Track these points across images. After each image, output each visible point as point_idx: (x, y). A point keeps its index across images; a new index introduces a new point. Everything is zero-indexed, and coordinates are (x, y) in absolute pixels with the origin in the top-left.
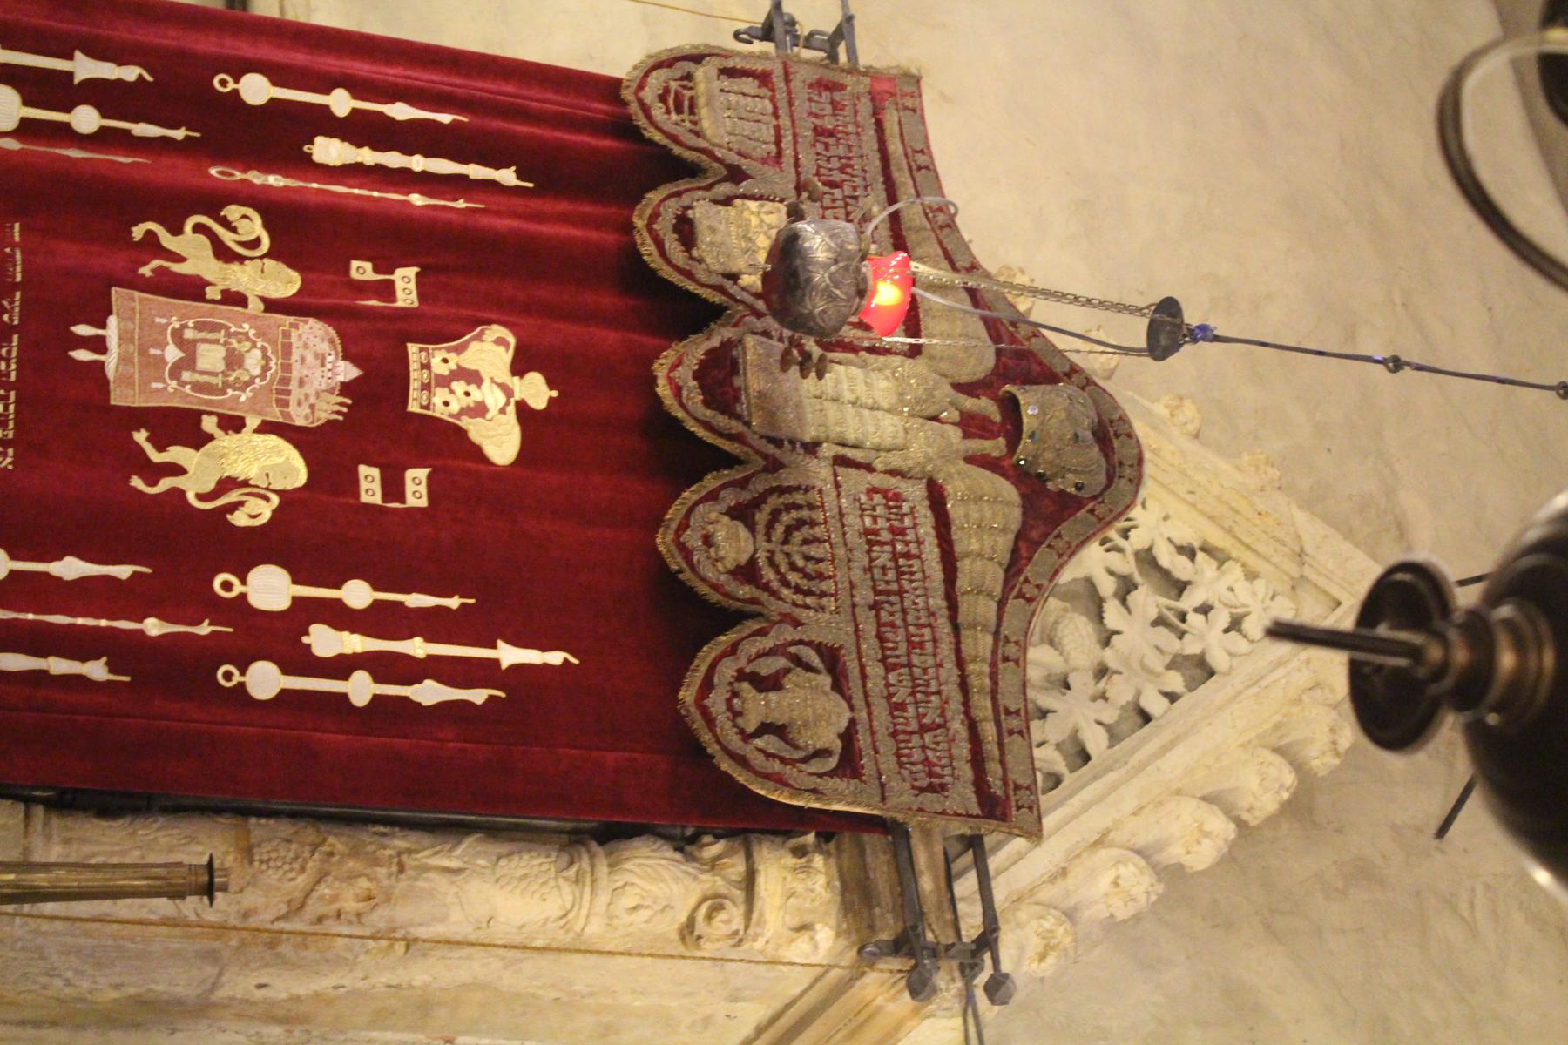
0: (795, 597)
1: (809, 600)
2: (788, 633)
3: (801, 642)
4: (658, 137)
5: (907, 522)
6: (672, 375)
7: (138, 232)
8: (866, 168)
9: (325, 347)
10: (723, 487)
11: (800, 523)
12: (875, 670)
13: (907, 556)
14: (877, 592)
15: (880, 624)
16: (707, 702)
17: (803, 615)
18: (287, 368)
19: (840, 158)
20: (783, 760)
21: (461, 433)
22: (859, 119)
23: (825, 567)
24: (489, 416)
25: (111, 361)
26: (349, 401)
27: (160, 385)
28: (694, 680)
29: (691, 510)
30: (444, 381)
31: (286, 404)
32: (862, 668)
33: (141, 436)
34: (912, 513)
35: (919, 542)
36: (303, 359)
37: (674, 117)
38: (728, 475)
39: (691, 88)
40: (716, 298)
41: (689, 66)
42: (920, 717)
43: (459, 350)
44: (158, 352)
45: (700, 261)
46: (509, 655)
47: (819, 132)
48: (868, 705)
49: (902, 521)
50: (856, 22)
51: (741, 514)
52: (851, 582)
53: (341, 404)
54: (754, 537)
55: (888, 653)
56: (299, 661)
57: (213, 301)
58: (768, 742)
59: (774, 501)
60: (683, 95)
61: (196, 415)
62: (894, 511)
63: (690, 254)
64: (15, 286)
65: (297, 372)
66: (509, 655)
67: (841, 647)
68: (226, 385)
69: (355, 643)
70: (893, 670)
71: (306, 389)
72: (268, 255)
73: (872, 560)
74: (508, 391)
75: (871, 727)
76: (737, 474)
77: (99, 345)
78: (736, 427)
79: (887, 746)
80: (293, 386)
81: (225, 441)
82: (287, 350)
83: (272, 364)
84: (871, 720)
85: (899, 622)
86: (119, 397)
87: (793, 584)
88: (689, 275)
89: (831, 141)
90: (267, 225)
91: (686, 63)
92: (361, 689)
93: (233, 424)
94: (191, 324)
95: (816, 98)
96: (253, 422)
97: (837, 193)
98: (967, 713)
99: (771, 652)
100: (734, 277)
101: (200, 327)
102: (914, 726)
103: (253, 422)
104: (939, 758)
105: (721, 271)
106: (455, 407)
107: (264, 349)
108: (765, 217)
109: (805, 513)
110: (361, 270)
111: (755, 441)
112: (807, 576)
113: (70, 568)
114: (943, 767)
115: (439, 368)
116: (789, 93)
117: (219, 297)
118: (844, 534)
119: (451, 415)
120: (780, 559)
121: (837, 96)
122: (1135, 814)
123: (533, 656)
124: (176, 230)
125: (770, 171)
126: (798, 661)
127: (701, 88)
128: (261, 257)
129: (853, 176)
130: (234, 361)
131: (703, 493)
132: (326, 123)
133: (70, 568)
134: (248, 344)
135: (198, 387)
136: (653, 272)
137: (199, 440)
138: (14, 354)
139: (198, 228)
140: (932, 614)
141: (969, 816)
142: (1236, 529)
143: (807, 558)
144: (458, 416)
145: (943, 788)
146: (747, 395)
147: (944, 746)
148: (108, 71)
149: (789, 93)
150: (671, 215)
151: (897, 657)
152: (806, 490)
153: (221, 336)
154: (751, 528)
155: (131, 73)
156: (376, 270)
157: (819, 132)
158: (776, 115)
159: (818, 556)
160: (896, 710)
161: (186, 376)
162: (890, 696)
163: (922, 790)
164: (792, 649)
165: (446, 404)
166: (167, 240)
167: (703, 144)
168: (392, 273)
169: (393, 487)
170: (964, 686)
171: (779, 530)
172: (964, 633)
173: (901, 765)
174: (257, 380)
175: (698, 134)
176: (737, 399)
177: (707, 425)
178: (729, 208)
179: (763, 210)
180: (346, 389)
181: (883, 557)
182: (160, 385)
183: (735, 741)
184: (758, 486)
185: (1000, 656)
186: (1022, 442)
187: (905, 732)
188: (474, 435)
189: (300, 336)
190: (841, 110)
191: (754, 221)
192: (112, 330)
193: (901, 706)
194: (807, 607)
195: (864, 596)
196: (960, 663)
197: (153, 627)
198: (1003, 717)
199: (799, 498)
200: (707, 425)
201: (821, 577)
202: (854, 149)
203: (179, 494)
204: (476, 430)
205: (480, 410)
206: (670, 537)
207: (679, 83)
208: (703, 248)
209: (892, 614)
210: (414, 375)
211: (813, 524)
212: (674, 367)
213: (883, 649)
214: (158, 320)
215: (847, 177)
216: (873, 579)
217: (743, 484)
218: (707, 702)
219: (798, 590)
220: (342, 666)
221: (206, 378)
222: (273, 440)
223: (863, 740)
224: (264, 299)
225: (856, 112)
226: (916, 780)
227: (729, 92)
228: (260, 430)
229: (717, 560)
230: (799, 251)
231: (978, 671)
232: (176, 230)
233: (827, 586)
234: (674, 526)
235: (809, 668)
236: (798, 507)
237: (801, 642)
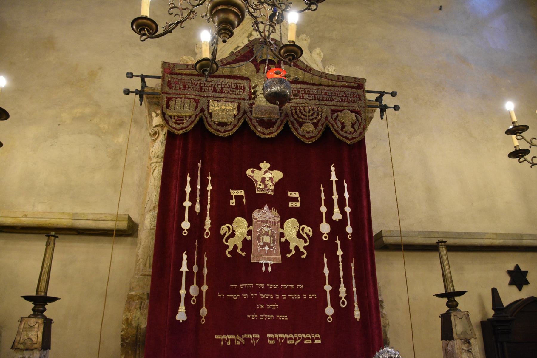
0: (319, 116)
1: (320, 113)
2: (330, 118)
3: (332, 117)
4: (192, 126)
5: (296, 89)
6: (266, 134)
7: (229, 256)
8: (195, 79)
9: (261, 212)
10: (294, 127)
11: (300, 112)
12: (334, 103)
13: (305, 91)
14: (315, 99)
15: (323, 100)
16: (350, 138)
17: (324, 115)
18: (267, 221)
19: (192, 85)
20: (360, 125)
21: (276, 183)
22: (179, 79)
23: (311, 108)
24: (273, 177)
25: (270, 262)
26: (273, 208)
27: (275, 251)
28: (345, 140)
29: (300, 135)
30: (266, 186)
31: (275, 222)
32: (334, 105)
33: (289, 256)
34: (293, 88)
35: (301, 88)
36: (264, 218)
37: (185, 121)
38: (290, 125)
39: (174, 116)
40: (242, 121)
41: (167, 116)
42: (343, 96)
43: (257, 182)
44: (267, 251)
45: (231, 122)
46: (334, 178)
47: (185, 88)
48: (343, 106)
49: (296, 91)
50: (143, 74)
51: (301, 124)
52: (313, 104)
53: (274, 210)
54: (306, 122)
55: (330, 100)
56: (343, 222)
57: (251, 238)
58: (356, 127)
59: (296, 116)
60: (177, 119)
61: (281, 243)
62: (293, 92)
63: (229, 124)
64: (254, 285)
65: (267, 219)
66: (334, 178)
67: (330, 109)
68: (272, 236)
69: (336, 210)
70: (333, 99)
71: (271, 218)
72: (231, 224)
73: (308, 99)
74: (266, 172)
75: (348, 106)
76: (290, 123)
77: (267, 265)
78: (279, 121)
79: (353, 105)
80: (270, 220)
81: (287, 237)
82: (262, 221)
83: (266, 225)
84: (346, 106)
85: (322, 96)
86: (278, 259)
87: (316, 116)
88: (235, 126)
89: (187, 86)
90: (224, 225)
91: (166, 117)
92: (348, 209)
93: (282, 235)
94: (259, 243)
95: (174, 88)
96: (281, 230)
97: (203, 88)
98: (341, 87)
99: (336, 123)
100: (235, 116)
101: (259, 241)
102: (346, 98)
103: (281, 230)
104: (352, 95)
105: (234, 118)
106: (271, 184)
107: (263, 226)
108: (215, 106)
109: (298, 111)
110: (233, 202)
111: (282, 118)
112: (314, 113)
113: (326, 271)
114: (354, 95)
115: (262, 186)
116: (173, 94)
117: (250, 237)
118: (301, 103)
119: (273, 185)
120: (311, 118)
121: (172, 82)
122: (318, 65)
123: (333, 173)
124: (227, 247)
125: (200, 103)
126: (336, 118)
127: (175, 114)
128: (232, 226)
129: (197, 83)
130: (267, 234)
131: (295, 131)
132: (192, 208)
133: (326, 271)
134: (262, 230)
135: (274, 242)
136: (234, 133)
137: (287, 243)
138: (271, 285)
139: (227, 241)
140: (318, 89)
141: (363, 92)
142: (246, 30)
143: (309, 112)
144: (273, 184)
145: (359, 95)
146: (269, 118)
147: (349, 93)
148: (185, 262)
149: (173, 94)
150: (218, 127)
151: (330, 98)
152: (291, 109)
153: (261, 237)
154: (304, 123)
155: (185, 257)
156: (232, 199)
157: (185, 88)
158: (181, 98)
159: (308, 110)
160: (343, 101)
161: (272, 245)
162: (339, 101)
163: (360, 99)
164: (334, 119)
165: (271, 186)
166: (231, 248)
167: (194, 116)
168: (232, 196)
170: (334, 86)
171: (302, 117)
172: (322, 83)
173: (356, 102)
174: (271, 229)
175: (190, 117)
176: (271, 120)
177: (278, 128)
178: (213, 113)
179: (213, 105)
180: (270, 208)
181: (307, 96)
182: (275, 251)
183: (357, 134)
184: (292, 119)
185: (325, 78)
186: (275, 61)
187: (348, 100)
188: (277, 181)
189: (259, 218)
190: (177, 82)
191: (217, 108)
192: (263, 262)
193: (342, 100)
194: (322, 114)
195: (317, 102)
196: (329, 86)
197: (340, 252)
198: (340, 80)
199: (294, 111)
200: (278, 128)
201: (313, 110)
202: (189, 81)
203: (305, 247)
204: (276, 180)
205: (271, 179)
206: (308, 141)
207: (173, 119)
208: (229, 121)
209: (320, 97)
210: (265, 192)
211: (300, 109)
212: (264, 134)
213: (329, 101)
214: (259, 251)
215: (198, 85)
216: (312, 99)
217: (292, 123)
218: (350, 138)
219: (318, 115)
220: (343, 212)
221: (272, 240)
222: (285, 225)
223: (352, 109)
224: (248, 227)
225: (177, 79)
226: (358, 100)
227: (175, 107)
228: (283, 228)
229: (313, 131)
230: (281, 92)
231: (331, 83)
232: (227, 247)
233: (316, 109)
234: (304, 139)
235: (337, 116)
236: (296, 112)
237: (332, 117)
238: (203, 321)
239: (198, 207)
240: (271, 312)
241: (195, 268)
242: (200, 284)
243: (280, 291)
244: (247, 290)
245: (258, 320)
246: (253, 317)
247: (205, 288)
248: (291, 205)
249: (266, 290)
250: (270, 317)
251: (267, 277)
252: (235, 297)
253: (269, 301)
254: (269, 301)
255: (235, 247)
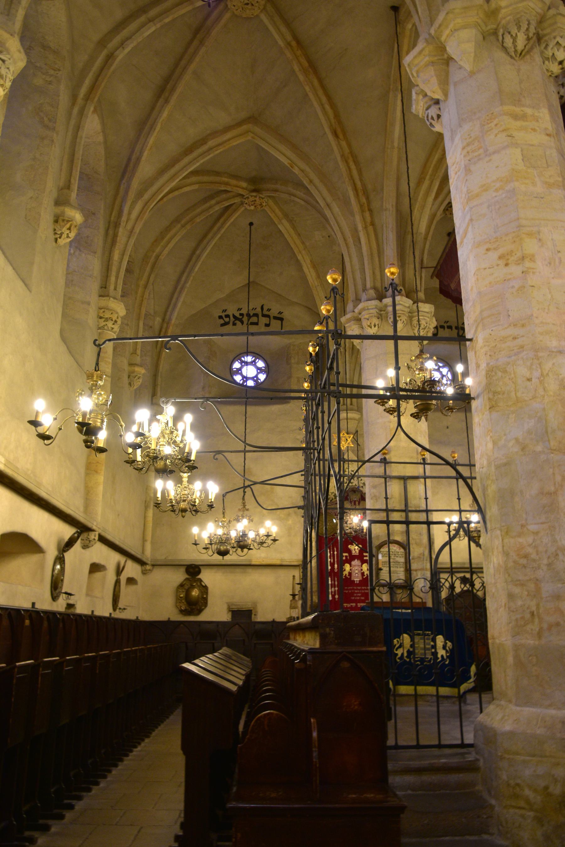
25: (358, 580)
30: (356, 552)
33: (364, 577)
81: (364, 570)
93: (362, 570)
110: (344, 558)
130: (356, 570)
132: (330, 561)
165: (357, 551)
169: (366, 556)
192: (355, 580)
238: (337, 600)
239: (332, 560)
240: (358, 596)
241: (333, 582)
242: (335, 587)
243: (361, 589)
244: (351, 589)
245: (354, 599)
246: (353, 598)
247: (336, 589)
248: (365, 558)
249: (357, 589)
250: (358, 598)
251: (357, 585)
252: (347, 592)
253: (358, 593)
254: (358, 593)
255: (346, 575)
